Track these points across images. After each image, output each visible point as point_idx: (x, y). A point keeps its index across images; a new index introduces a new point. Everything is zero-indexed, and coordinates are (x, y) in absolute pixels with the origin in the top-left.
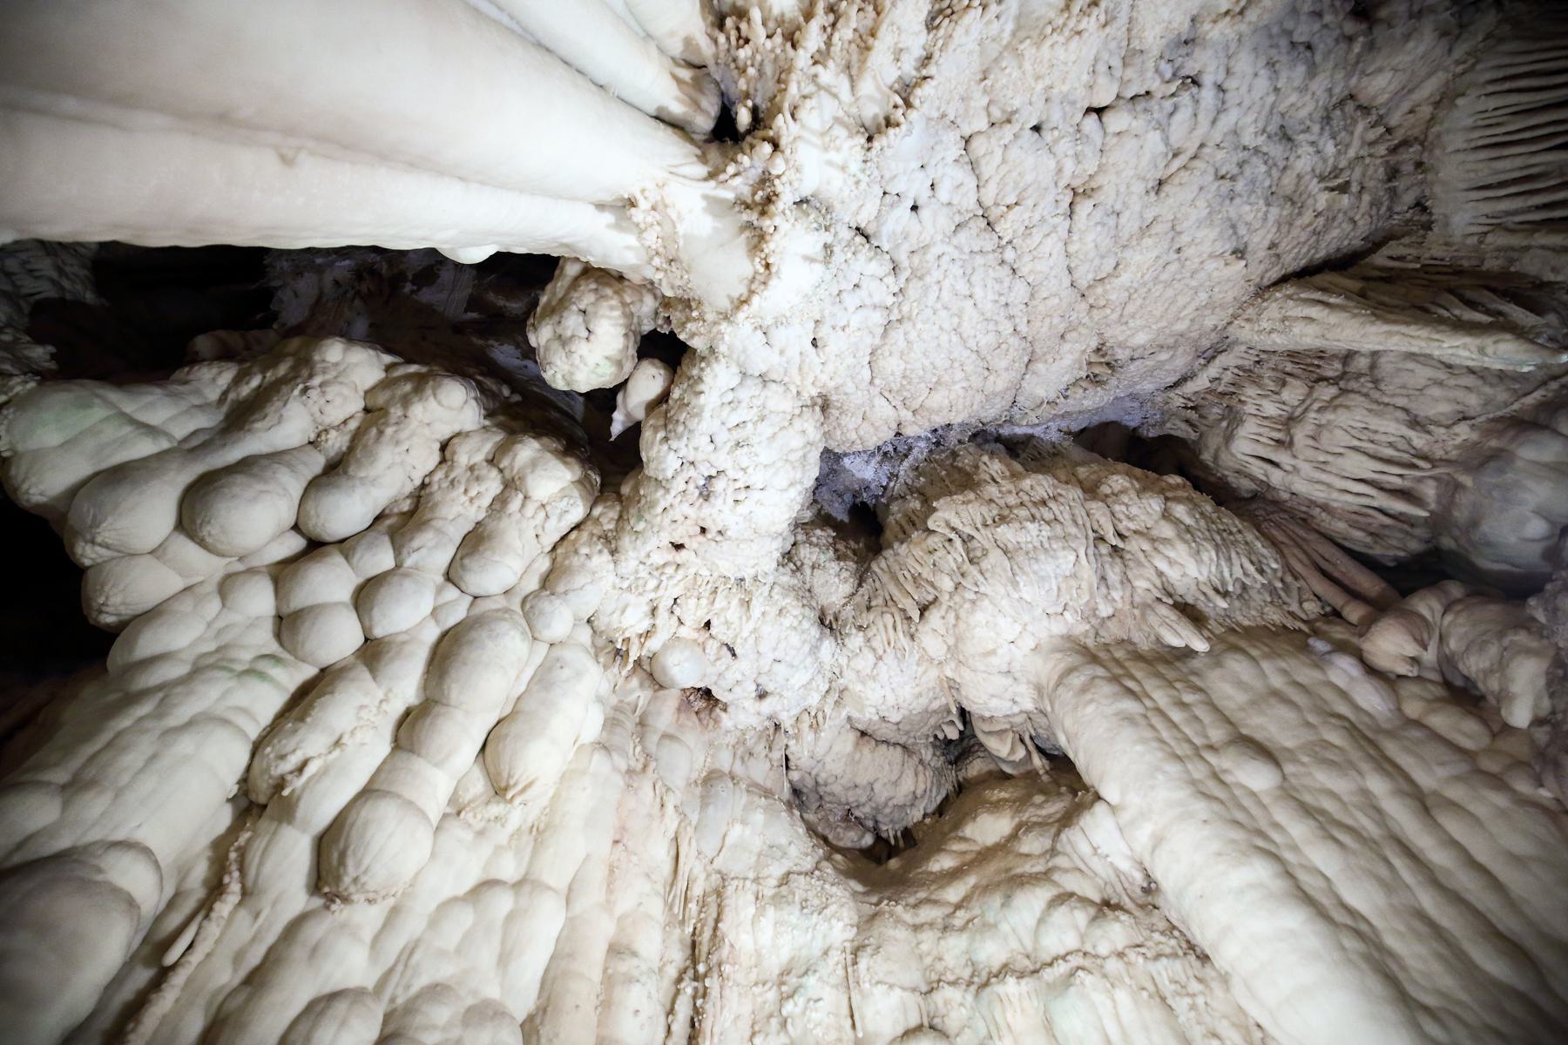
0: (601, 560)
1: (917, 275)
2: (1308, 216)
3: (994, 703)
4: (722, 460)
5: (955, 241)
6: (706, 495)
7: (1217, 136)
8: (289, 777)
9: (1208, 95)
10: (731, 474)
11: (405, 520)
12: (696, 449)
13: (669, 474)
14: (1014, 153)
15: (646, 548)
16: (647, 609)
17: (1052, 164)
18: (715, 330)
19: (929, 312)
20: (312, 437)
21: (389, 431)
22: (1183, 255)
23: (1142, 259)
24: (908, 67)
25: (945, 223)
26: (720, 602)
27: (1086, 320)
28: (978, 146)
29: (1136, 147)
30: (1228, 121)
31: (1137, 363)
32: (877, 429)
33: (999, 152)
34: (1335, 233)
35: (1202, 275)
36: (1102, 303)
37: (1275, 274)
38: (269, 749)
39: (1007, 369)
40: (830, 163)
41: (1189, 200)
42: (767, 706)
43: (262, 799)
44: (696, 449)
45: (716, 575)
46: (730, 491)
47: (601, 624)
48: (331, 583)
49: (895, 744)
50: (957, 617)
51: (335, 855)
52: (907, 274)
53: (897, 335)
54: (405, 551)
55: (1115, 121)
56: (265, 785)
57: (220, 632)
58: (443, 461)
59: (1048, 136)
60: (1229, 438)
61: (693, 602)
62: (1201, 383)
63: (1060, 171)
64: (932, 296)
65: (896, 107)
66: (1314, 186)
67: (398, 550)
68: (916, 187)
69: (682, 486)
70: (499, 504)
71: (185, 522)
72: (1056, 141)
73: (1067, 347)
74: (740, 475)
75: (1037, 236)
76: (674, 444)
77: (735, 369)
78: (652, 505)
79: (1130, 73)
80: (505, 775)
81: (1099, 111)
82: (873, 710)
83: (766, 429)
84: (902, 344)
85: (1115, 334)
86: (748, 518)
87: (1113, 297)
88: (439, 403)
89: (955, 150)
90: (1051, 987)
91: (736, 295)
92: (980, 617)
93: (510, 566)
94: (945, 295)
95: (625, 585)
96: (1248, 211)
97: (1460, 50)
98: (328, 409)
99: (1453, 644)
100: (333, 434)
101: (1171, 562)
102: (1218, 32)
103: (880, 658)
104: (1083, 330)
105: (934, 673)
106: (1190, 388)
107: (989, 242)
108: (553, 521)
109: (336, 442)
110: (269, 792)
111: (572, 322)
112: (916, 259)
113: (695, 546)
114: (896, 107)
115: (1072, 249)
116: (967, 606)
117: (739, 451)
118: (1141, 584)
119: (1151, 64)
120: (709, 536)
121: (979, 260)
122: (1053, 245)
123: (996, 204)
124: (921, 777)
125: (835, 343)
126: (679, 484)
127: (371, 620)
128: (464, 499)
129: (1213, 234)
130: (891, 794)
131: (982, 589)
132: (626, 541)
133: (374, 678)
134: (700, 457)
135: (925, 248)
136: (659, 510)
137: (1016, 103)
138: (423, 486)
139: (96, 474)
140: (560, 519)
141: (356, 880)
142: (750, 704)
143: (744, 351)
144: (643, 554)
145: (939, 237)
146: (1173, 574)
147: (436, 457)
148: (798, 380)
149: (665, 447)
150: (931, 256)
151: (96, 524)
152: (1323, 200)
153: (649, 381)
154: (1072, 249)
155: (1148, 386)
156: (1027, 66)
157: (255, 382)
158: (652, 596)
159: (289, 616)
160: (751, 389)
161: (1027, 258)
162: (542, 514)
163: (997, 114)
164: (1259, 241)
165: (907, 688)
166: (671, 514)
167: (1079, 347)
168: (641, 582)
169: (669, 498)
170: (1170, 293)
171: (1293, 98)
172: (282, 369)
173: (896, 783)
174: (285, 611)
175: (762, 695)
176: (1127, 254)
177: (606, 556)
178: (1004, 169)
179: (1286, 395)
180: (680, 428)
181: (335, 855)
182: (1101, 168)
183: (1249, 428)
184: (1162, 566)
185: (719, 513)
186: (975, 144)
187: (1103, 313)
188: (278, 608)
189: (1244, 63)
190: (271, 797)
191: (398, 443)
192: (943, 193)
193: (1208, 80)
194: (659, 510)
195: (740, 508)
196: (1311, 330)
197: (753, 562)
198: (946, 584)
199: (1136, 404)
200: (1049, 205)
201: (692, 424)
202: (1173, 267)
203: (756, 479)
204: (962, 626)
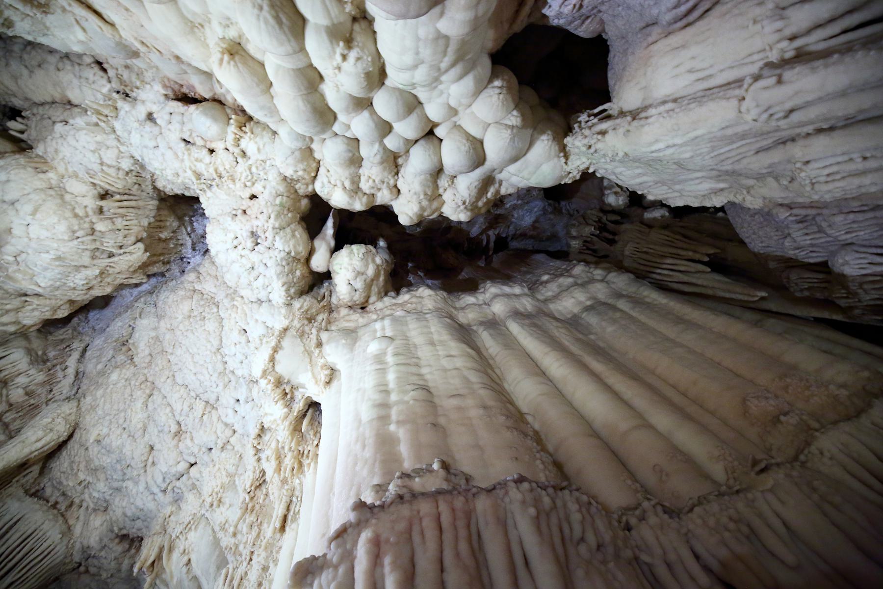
0: (289, 172)
1: (222, 374)
2: (82, 467)
4: (255, 257)
5: (216, 394)
6: (253, 234)
7: (142, 478)
8: (346, 52)
9: (156, 490)
10: (246, 252)
11: (393, 162)
12: (271, 257)
13: (277, 238)
14: (213, 438)
15: (269, 189)
16: (249, 153)
17: (196, 442)
18: (291, 317)
19: (208, 360)
20: (455, 180)
21: (422, 197)
22: (120, 430)
23: (137, 417)
24: (263, 456)
25: (223, 400)
26: (212, 170)
27: (146, 371)
28: (228, 432)
29: (168, 460)
30: (142, 487)
31: (110, 356)
32: (209, 274)
34: (66, 465)
35: (106, 424)
36: (143, 386)
37: (77, 436)
38: (370, 59)
39: (165, 334)
40: (272, 415)
41: (134, 451)
42: (141, 111)
43: (357, 27)
44: (271, 257)
45: (225, 187)
46: (243, 242)
47: (267, 136)
48: (405, 128)
50: (76, 216)
51: (284, 20)
52: (227, 372)
53: (216, 343)
54: (381, 151)
55: (183, 466)
56: (359, 39)
57: (442, 93)
58: (396, 186)
59: (204, 449)
60: (29, 351)
61: (227, 167)
62: (72, 362)
63: (192, 440)
65: (259, 444)
66: (89, 479)
67: (385, 148)
68: (242, 409)
69: (267, 234)
70: (355, 181)
71: (479, 145)
72: (200, 450)
73: (147, 352)
74: (243, 253)
75: (186, 408)
76: (283, 254)
77: (274, 302)
78: (278, 216)
79: (190, 482)
80: (239, 65)
81: (192, 465)
83: (244, 281)
84: (212, 340)
85: (128, 372)
86: (226, 231)
87: (139, 393)
88: (407, 215)
89: (236, 428)
91: (280, 352)
92: (62, 229)
93: (329, 152)
95: (268, 163)
96: (106, 461)
97: (78, 546)
98: (452, 197)
100: (446, 185)
102: (168, 510)
104: (144, 365)
105: (61, 169)
106: (76, 355)
107: (204, 397)
108: (325, 180)
109: (443, 182)
110: (354, 35)
111: (359, 284)
112: (227, 380)
113: (244, 202)
114: (259, 444)
115: (168, 409)
116: (76, 228)
117: (250, 265)
119: (184, 489)
120: (239, 212)
121: (201, 390)
122: (177, 407)
123: (210, 412)
125: (235, 336)
126: (270, 234)
127: (373, 120)
128: (373, 177)
129: (114, 445)
131: (75, 242)
132: (281, 188)
133: (350, 95)
134: (267, 255)
135: (225, 386)
136: (272, 216)
137: (223, 455)
138: (397, 173)
139: (525, 155)
140: (323, 183)
141: (261, 8)
142: (154, 108)
143: (273, 315)
144: (268, 186)
147: (399, 186)
148: (245, 307)
149: (287, 250)
150: (221, 385)
151: (512, 139)
152: (82, 476)
153: (318, 263)
154: (168, 409)
155: (98, 342)
157: (489, 195)
158: (250, 162)
159: (415, 108)
160: (263, 295)
161: (185, 396)
162: (333, 182)
163: (229, 447)
164: (94, 450)
165: (68, 155)
166: (265, 216)
167: (141, 355)
168: (261, 168)
169: (271, 226)
170: (115, 407)
171: (124, 504)
172: (480, 204)
174: (418, 111)
175: (150, 117)
176: (145, 415)
177: (287, 174)
178: (214, 429)
179: (21, 391)
180: (284, 263)
181: (284, 20)
182: (177, 446)
186: (231, 432)
187: (139, 381)
188: (423, 108)
189: (151, 505)
190: (352, 30)
191: (415, 194)
192: (230, 412)
193: (160, 495)
194: (272, 216)
195: (233, 236)
196: (34, 438)
197: (211, 201)
198: (100, 227)
199: (97, 327)
200: (189, 423)
201: (279, 269)
202: (121, 421)
203: (234, 255)
204: (68, 214)
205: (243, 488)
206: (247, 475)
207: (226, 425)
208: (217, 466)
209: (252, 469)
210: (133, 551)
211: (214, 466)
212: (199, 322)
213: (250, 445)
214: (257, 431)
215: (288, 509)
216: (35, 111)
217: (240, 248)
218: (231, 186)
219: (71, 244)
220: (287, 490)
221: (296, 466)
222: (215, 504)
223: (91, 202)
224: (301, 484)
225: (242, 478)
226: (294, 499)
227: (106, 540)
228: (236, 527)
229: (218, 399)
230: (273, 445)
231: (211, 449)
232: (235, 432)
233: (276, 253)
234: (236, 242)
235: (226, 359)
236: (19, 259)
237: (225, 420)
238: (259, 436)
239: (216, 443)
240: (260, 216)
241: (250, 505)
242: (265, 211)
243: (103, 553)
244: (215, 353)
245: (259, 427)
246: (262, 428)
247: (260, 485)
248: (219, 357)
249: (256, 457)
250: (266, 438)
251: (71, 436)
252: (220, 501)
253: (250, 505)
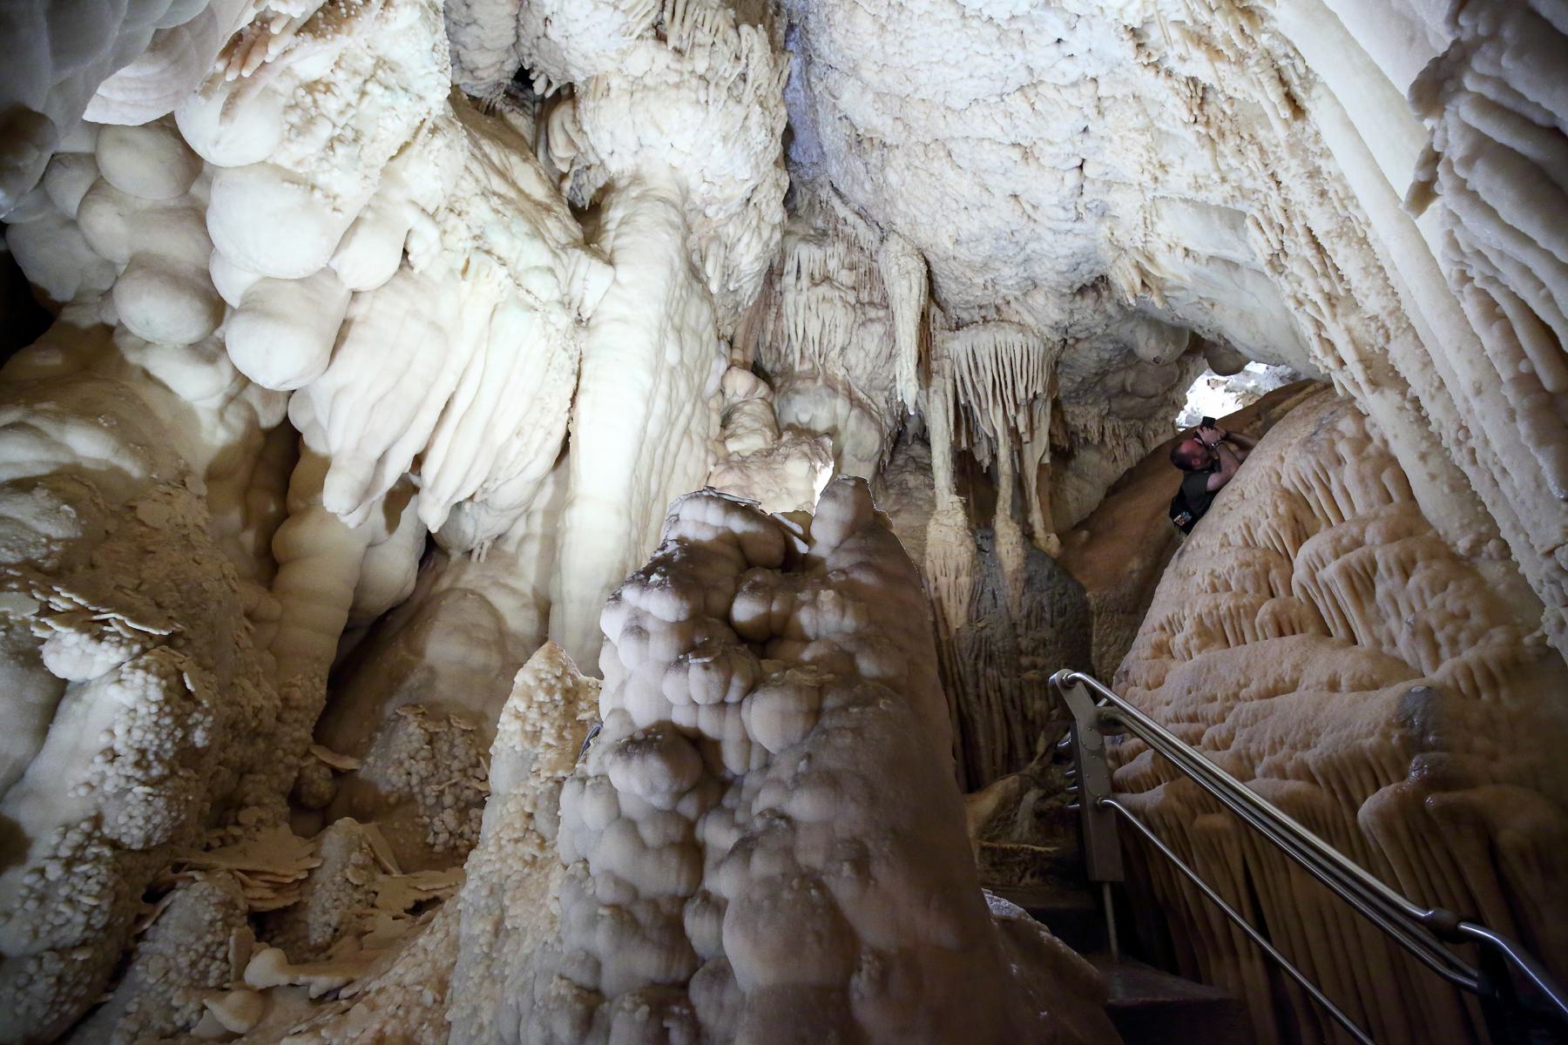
1: (1002, 36)
2: (969, 274)
3: (605, 136)
7: (1038, 230)
9: (1069, 226)
14: (1075, 114)
17: (1058, 140)
22: (964, 215)
23: (964, 186)
24: (1171, 63)
25: (1039, 63)
27: (913, 139)
28: (1088, 89)
29: (1048, 189)
30: (1049, 237)
31: (863, 168)
33: (1079, 104)
34: (953, 286)
35: (944, 222)
36: (931, 155)
37: (931, 258)
39: (882, 81)
41: (1003, 215)
49: (518, 36)
50: (677, 86)
55: (1072, 179)
59: (1078, 138)
60: (805, 239)
62: (841, 211)
63: (1051, 143)
64: (978, 47)
65: (1149, 55)
66: (989, 276)
68: (1075, 44)
72: (1073, 143)
73: (890, 121)
75: (1005, 122)
79: (1098, 184)
81: (1081, 167)
85: (898, 159)
87: (936, 164)
89: (1091, 74)
90: (519, 300)
92: (689, 112)
94: (980, 59)
96: (985, 249)
97: (1046, 330)
99: (747, 408)
101: (748, 245)
102: (1104, 230)
104: (905, 134)
105: (610, 66)
106: (836, 202)
112: (1016, 36)
115: (986, 144)
116: (693, 96)
118: (731, 229)
119: (1100, 197)
121: (999, 84)
122: (993, 131)
124: (492, 70)
129: (975, 230)
130: (470, 47)
131: (711, 108)
135: (1023, 45)
137: (1109, 118)
145: (1029, 57)
146: (741, 248)
152: (979, 281)
154: (986, 144)
155: (834, 169)
156: (1134, 135)
161: (986, 112)
163: (1106, 104)
164: (962, 252)
167: (888, 131)
170: (932, 201)
171: (1049, 265)
173: (482, 47)
176: (969, 176)
179: (844, 272)
182: (1042, 166)
183: (818, 254)
184: (745, 239)
186: (1091, 86)
187: (921, 155)
189: (1079, 243)
192: (1065, 65)
193: (1078, 225)
196: (905, 291)
198: (701, 67)
199: (815, 159)
200: (1025, 133)
202: (954, 206)
204: (673, 93)
205: (1179, 123)
206: (1169, 105)
207: (1075, 84)
208: (1116, 138)
209: (1171, 93)
210: (1105, 293)
211: (1111, 140)
212: (903, 17)
213: (1138, 70)
214: (1131, 44)
215: (1283, 82)
216: (526, 51)
219: (712, 115)
220: (1258, 63)
221: (1243, 22)
222: (1159, 173)
223: (664, 57)
224: (1275, 34)
225: (1165, 116)
226: (1283, 63)
227: (1067, 306)
228: (1218, 169)
229: (1030, 70)
230: (1174, 34)
231: (1085, 130)
232: (1095, 80)
235: (986, 13)
237: (1067, 81)
238: (1139, 46)
239: (1086, 117)
241: (1213, 133)
243: (1076, 317)
244: (964, 25)
245: (1126, 36)
246: (1134, 32)
247: (1202, 98)
248: (975, 23)
249: (1162, 74)
250: (1154, 36)
251: (927, 263)
252: (1162, 166)
253: (1213, 133)
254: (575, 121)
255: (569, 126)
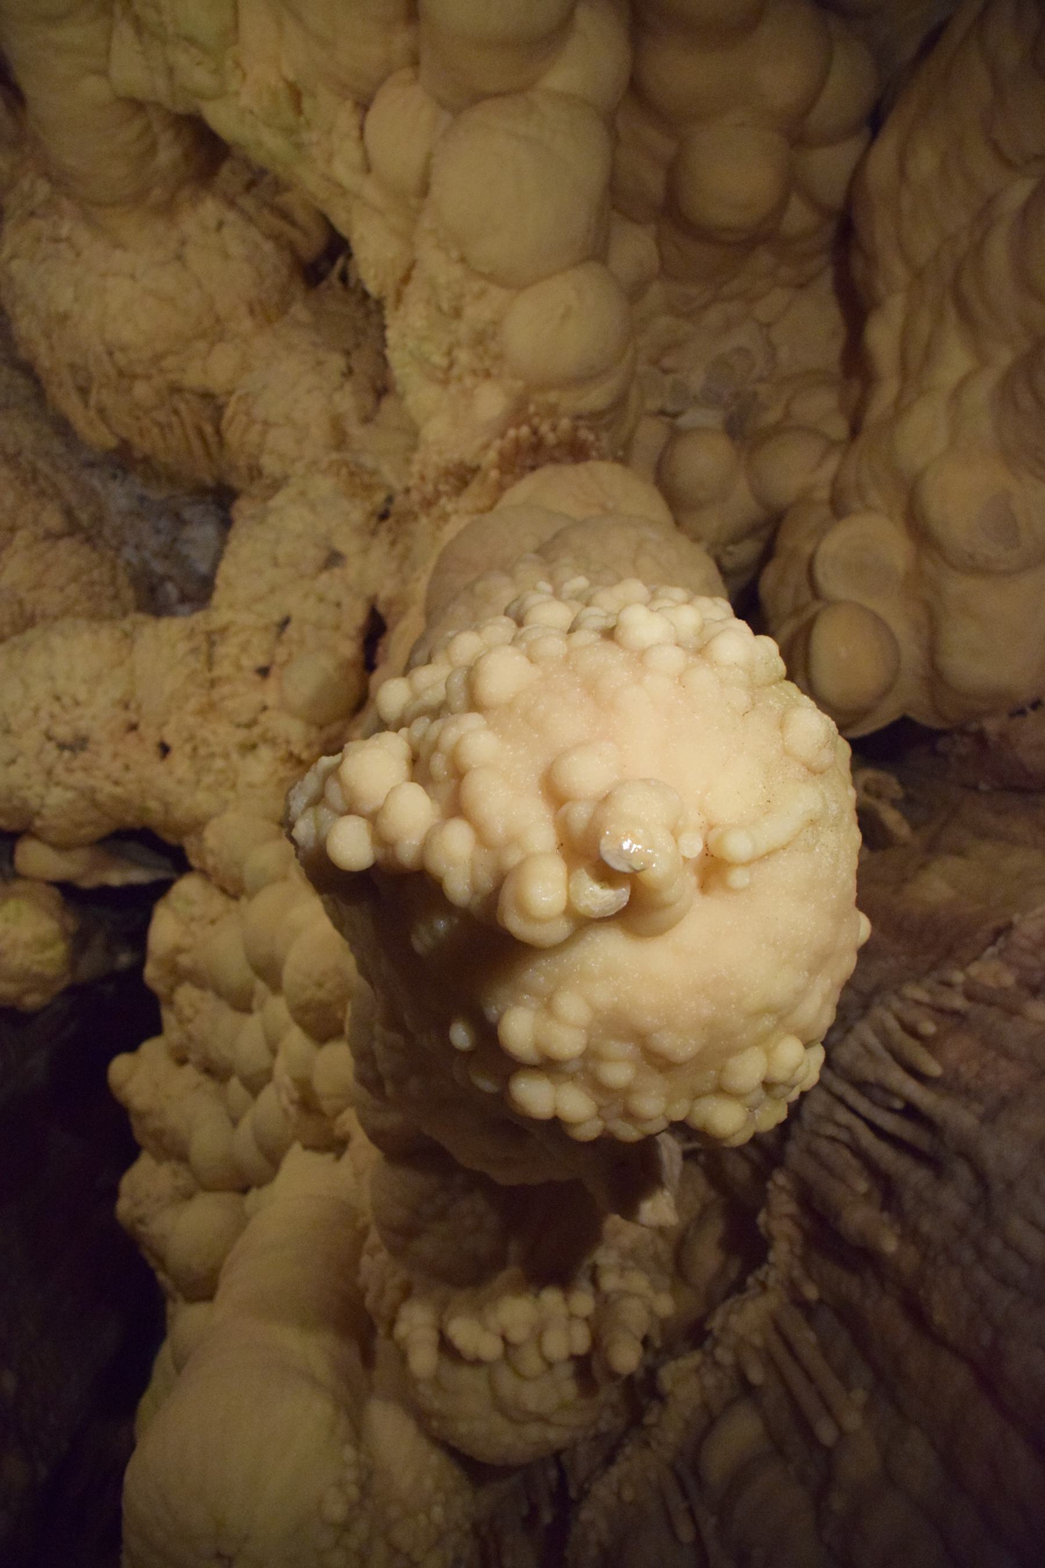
3: (236, 249)
4: (31, 740)
6: (78, 744)
10: (43, 726)
13: (70, 795)
42: (348, 545)
74: (43, 714)
78: (117, 800)
82: (337, 397)
86: (97, 679)
95: (231, 795)
103: (266, 423)
117: (14, 727)
120: (133, 717)
126: (79, 778)
136: (118, 790)
142: (352, 570)
158: (235, 756)
175: (334, 559)
185: (97, 715)
195: (82, 695)
203: (40, 691)
217: (56, 709)
218: (193, 704)
223: (193, 378)
233: (38, 789)
234: (67, 700)
236: (63, 246)
240: (118, 764)
242: (131, 776)
254: (291, 247)
255: (295, 235)
